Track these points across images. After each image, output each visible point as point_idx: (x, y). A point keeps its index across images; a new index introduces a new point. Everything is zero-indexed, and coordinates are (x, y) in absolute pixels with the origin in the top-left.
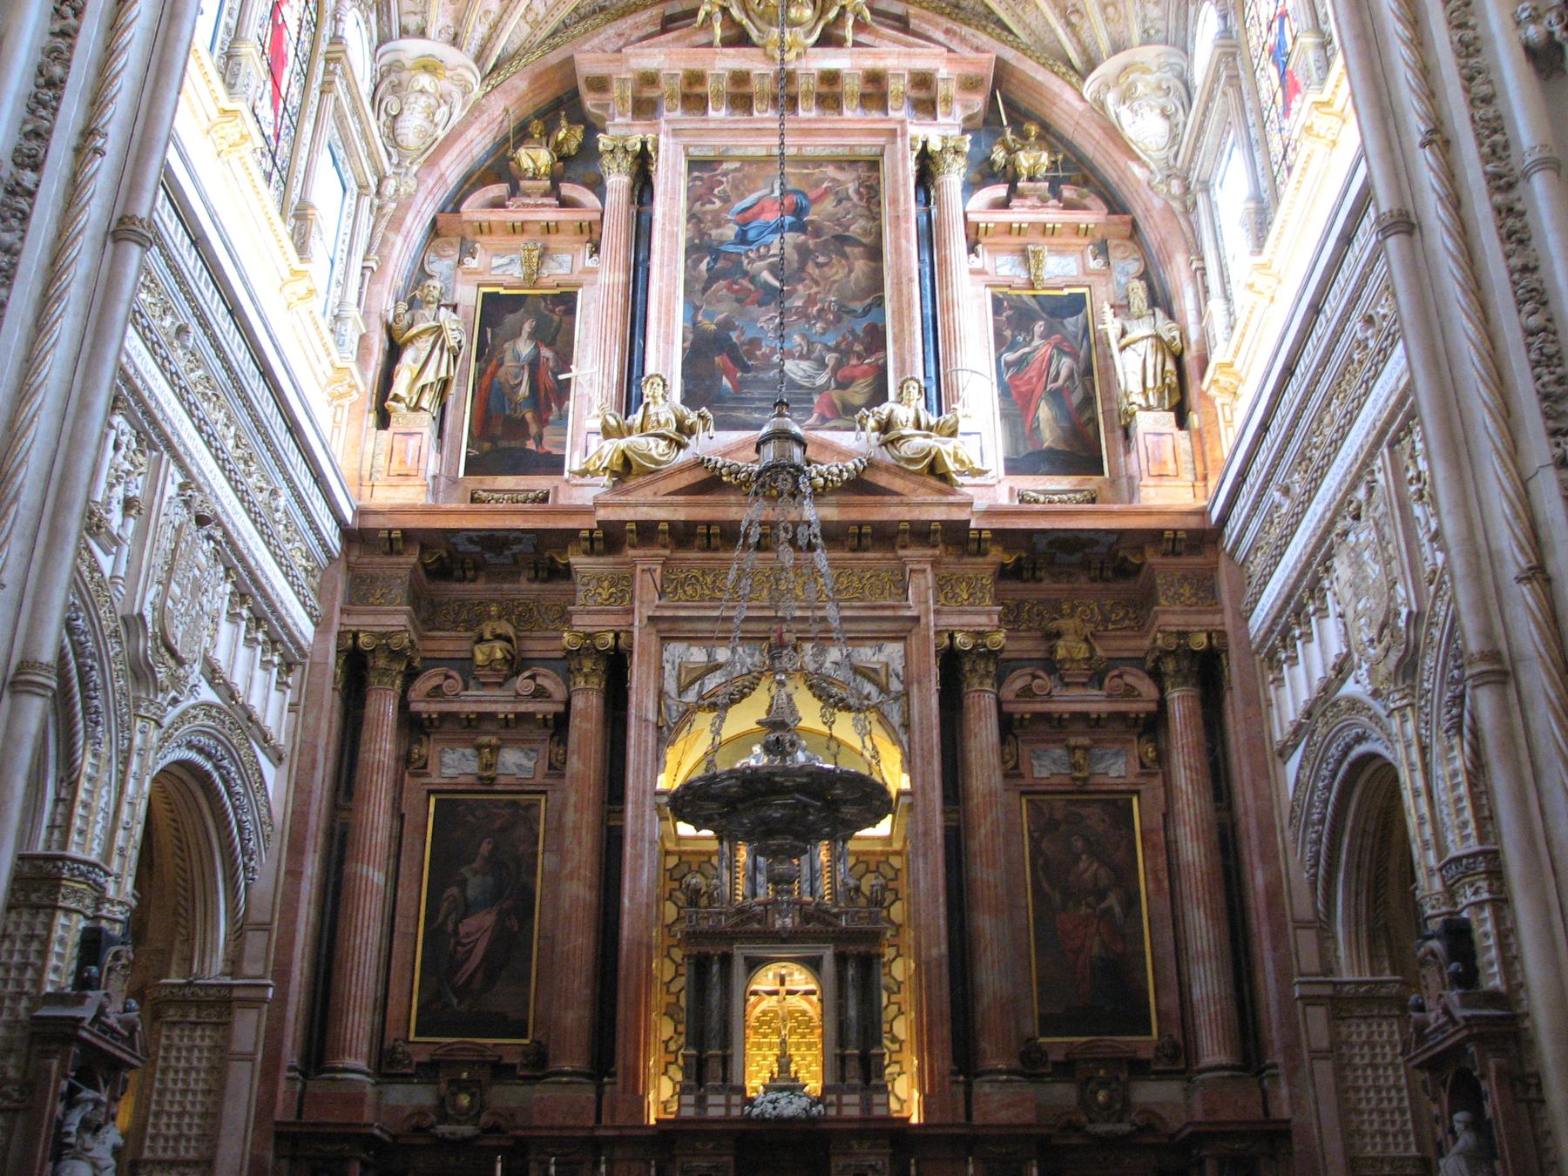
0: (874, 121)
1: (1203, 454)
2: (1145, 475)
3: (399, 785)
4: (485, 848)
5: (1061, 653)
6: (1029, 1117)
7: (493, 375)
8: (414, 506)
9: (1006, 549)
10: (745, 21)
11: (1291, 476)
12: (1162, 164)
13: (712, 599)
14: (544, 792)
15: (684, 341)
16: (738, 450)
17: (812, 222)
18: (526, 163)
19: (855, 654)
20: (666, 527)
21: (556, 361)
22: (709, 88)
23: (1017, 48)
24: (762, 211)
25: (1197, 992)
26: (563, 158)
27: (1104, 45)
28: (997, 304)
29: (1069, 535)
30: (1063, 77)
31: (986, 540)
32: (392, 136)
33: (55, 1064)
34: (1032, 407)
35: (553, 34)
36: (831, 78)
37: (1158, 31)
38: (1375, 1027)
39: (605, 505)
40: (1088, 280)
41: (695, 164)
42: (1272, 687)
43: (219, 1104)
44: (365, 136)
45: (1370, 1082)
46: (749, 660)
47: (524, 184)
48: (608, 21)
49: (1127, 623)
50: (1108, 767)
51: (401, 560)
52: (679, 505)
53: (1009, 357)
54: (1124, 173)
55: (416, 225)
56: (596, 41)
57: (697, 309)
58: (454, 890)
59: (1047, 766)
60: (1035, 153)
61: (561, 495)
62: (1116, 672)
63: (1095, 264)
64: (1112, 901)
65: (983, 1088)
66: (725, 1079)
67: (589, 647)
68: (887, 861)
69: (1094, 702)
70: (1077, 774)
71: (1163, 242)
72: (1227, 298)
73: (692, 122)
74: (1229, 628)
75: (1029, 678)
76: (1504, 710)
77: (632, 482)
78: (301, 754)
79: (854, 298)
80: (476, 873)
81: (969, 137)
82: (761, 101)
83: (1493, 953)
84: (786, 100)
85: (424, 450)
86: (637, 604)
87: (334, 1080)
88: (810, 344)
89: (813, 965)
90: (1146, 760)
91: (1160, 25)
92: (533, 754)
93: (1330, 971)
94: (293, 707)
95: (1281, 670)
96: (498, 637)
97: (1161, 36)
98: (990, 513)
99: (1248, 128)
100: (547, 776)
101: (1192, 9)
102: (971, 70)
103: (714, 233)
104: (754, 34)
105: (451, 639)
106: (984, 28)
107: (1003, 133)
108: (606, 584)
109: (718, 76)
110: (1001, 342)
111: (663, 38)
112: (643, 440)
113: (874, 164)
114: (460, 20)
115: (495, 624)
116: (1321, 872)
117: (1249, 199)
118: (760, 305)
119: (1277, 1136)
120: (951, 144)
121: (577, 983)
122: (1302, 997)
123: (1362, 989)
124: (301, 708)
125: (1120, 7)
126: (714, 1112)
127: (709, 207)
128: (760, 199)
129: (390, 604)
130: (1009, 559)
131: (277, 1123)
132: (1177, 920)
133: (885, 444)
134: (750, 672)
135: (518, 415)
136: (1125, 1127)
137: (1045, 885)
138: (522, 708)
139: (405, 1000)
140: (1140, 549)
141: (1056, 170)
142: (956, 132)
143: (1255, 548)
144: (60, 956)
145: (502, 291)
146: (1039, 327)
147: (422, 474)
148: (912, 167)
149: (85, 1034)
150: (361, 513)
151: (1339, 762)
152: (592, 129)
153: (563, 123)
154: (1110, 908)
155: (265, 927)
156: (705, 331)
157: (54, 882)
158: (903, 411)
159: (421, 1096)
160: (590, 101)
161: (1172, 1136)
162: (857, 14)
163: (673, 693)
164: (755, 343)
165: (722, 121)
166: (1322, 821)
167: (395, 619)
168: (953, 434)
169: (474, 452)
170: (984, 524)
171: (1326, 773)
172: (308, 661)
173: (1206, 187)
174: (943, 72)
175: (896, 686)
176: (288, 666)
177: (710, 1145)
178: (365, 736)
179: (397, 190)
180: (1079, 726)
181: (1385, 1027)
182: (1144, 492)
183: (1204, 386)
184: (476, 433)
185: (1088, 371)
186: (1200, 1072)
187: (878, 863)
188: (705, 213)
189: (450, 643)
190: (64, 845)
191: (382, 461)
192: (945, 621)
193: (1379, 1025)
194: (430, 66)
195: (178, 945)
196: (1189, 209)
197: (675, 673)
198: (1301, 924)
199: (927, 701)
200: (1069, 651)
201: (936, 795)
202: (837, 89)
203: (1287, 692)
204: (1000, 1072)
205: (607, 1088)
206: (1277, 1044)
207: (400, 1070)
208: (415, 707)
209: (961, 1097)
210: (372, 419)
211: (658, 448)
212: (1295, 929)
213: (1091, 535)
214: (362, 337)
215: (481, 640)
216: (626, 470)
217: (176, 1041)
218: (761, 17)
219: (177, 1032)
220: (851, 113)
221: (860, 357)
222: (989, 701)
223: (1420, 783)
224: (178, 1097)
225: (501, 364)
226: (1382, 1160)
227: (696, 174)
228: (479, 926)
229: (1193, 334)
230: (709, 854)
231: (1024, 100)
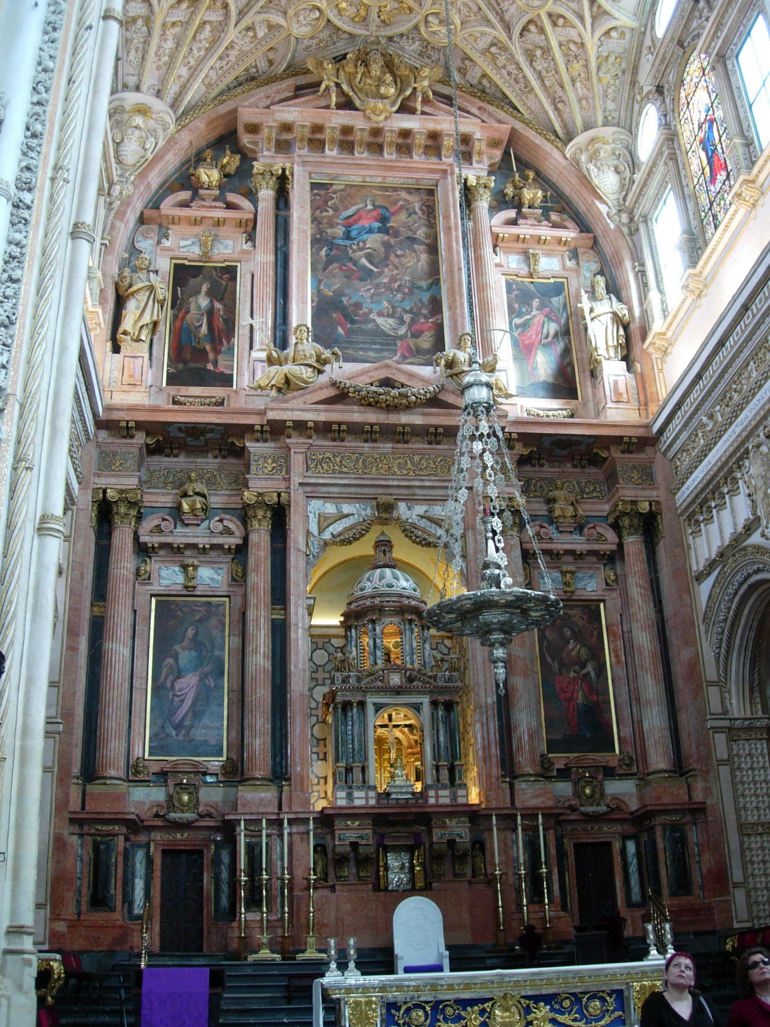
0: (433, 164)
1: (644, 389)
2: (609, 400)
4: (190, 633)
5: (557, 513)
6: (550, 803)
7: (183, 318)
8: (144, 405)
9: (525, 445)
10: (351, 94)
11: (715, 407)
12: (615, 203)
13: (340, 472)
14: (229, 596)
15: (312, 302)
16: (358, 376)
17: (392, 227)
18: (204, 178)
19: (431, 510)
20: (310, 424)
21: (225, 311)
22: (327, 135)
23: (523, 122)
24: (360, 219)
25: (646, 726)
26: (226, 176)
27: (579, 124)
28: (509, 285)
29: (565, 438)
30: (552, 142)
31: (514, 440)
34: (533, 353)
35: (221, 93)
36: (406, 134)
37: (613, 118)
38: (753, 746)
39: (273, 409)
40: (565, 274)
41: (314, 186)
42: (691, 537)
45: (751, 779)
46: (363, 513)
47: (201, 192)
48: (258, 87)
49: (595, 494)
50: (586, 585)
51: (133, 441)
52: (320, 410)
53: (517, 321)
54: (591, 208)
55: (132, 217)
56: (253, 99)
57: (320, 281)
58: (170, 661)
60: (533, 191)
61: (232, 400)
62: (592, 525)
63: (570, 264)
64: (589, 668)
65: (520, 785)
66: (364, 781)
67: (261, 503)
68: (443, 643)
69: (578, 543)
70: (568, 589)
71: (617, 253)
72: (661, 291)
73: (315, 157)
74: (660, 499)
75: (538, 528)
77: (290, 395)
78: (73, 570)
79: (420, 279)
80: (184, 649)
81: (494, 178)
82: (361, 146)
84: (376, 148)
85: (145, 369)
86: (292, 474)
87: (105, 784)
88: (394, 307)
89: (417, 708)
90: (609, 581)
91: (616, 114)
92: (220, 571)
93: (728, 711)
95: (699, 525)
96: (197, 494)
97: (616, 121)
99: (682, 187)
100: (230, 585)
101: (636, 107)
102: (496, 135)
103: (329, 231)
104: (357, 103)
105: (163, 494)
106: (502, 107)
107: (514, 177)
108: (270, 461)
109: (333, 128)
110: (512, 311)
111: (297, 101)
112: (297, 367)
113: (431, 192)
114: (163, 81)
115: (195, 485)
116: (723, 651)
117: (684, 232)
118: (361, 280)
119: (698, 810)
120: (482, 181)
122: (712, 728)
123: (747, 723)
124: (72, 539)
125: (591, 101)
126: (357, 803)
127: (325, 214)
128: (358, 211)
129: (127, 470)
130: (526, 452)
131: (70, 812)
133: (451, 376)
134: (364, 521)
135: (201, 346)
136: (603, 809)
137: (549, 660)
138: (215, 541)
139: (142, 729)
140: (608, 449)
141: (546, 202)
142: (486, 174)
143: (682, 450)
145: (187, 263)
146: (536, 303)
147: (144, 384)
148: (458, 195)
150: (108, 409)
151: (741, 585)
152: (247, 158)
153: (228, 152)
154: (588, 673)
156: (326, 297)
159: (156, 794)
160: (245, 139)
161: (632, 813)
162: (424, 94)
163: (316, 532)
164: (358, 306)
165: (334, 158)
166: (725, 620)
167: (132, 482)
169: (172, 370)
170: (513, 429)
171: (732, 591)
172: (75, 507)
173: (646, 222)
174: (478, 135)
177: (357, 823)
178: (113, 558)
179: (121, 193)
180: (570, 559)
181: (759, 746)
182: (609, 412)
183: (645, 347)
184: (172, 356)
186: (649, 774)
187: (438, 643)
188: (323, 218)
189: (164, 498)
191: (116, 374)
193: (756, 744)
194: (143, 110)
196: (634, 232)
197: (316, 520)
198: (711, 684)
200: (562, 510)
202: (409, 141)
203: (701, 541)
204: (530, 775)
205: (285, 788)
206: (695, 758)
207: (141, 777)
208: (143, 539)
209: (508, 791)
210: (109, 345)
212: (707, 686)
213: (578, 438)
214: (101, 290)
215: (185, 495)
216: (288, 385)
218: (361, 90)
220: (418, 157)
221: (425, 317)
225: (187, 312)
226: (758, 824)
227: (316, 191)
228: (189, 684)
229: (637, 312)
230: (330, 637)
231: (525, 157)
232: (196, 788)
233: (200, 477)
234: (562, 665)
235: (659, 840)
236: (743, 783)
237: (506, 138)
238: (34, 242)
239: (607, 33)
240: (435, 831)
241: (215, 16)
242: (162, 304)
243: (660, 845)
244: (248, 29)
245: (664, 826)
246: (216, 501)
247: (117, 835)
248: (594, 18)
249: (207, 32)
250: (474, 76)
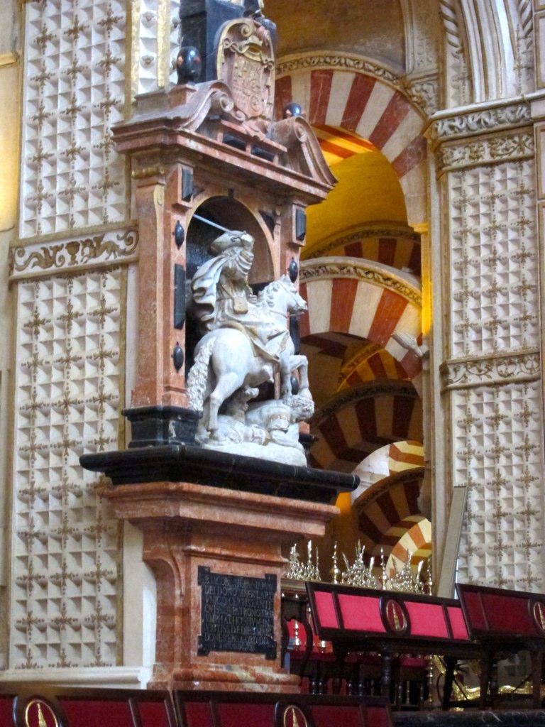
33: (158, 193)
144: (149, 42)
149: (193, 145)
195: (450, 61)
217: (470, 192)
219: (469, 180)
224: (484, 270)
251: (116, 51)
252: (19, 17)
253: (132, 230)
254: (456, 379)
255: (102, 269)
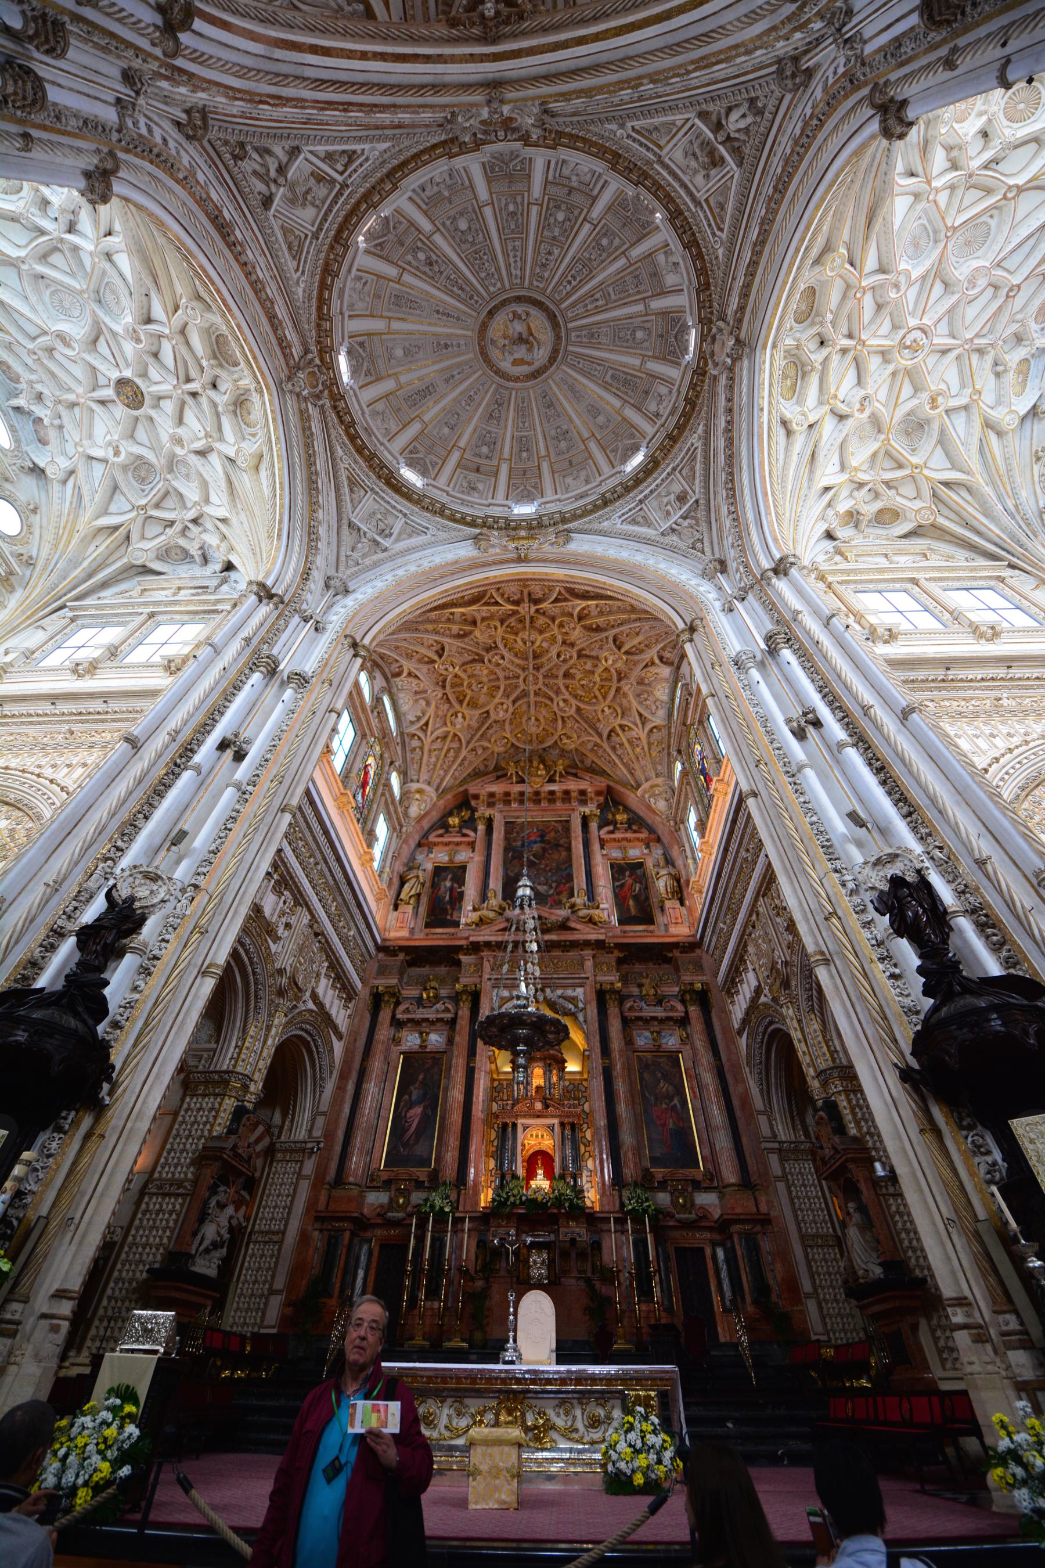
3: (388, 1050)
4: (421, 1077)
9: (620, 951)
28: (612, 865)
32: (406, 814)
43: (292, 1202)
44: (396, 812)
55: (413, 844)
59: (643, 1039)
64: (676, 1101)
67: (465, 991)
69: (659, 1012)
73: (507, 808)
76: (832, 977)
83: (850, 1117)
84: (537, 802)
94: (349, 1016)
98: (613, 937)
113: (568, 821)
119: (765, 1221)
121: (453, 1141)
130: (621, 955)
132: (704, 1109)
136: (693, 1216)
143: (716, 948)
151: (764, 1034)
155: (323, 1114)
157: (227, 1083)
158: (579, 900)
160: (473, 803)
167: (394, 981)
168: (598, 907)
175: (581, 1005)
176: (349, 999)
185: (646, 888)
186: (725, 1187)
190: (234, 1066)
192: (598, 978)
194: (420, 791)
196: (678, 830)
198: (760, 1113)
199: (592, 1011)
201: (598, 1051)
203: (737, 1007)
211: (491, 915)
215: (425, 989)
216: (481, 922)
220: (559, 804)
222: (617, 1010)
223: (800, 1036)
229: (683, 873)
232: (409, 1194)
233: (436, 978)
234: (656, 1098)
235: (738, 1247)
236: (799, 1198)
237: (605, 789)
238: (248, 811)
239: (651, 731)
240: (562, 1230)
241: (455, 745)
242: (423, 884)
243: (739, 1253)
244: (474, 750)
245: (739, 1233)
246: (444, 992)
247: (345, 1230)
248: (643, 724)
249: (452, 753)
250: (588, 763)
251: (211, 1119)
252: (183, 1100)
253: (195, 1182)
254: (254, 1237)
255: (179, 1195)
